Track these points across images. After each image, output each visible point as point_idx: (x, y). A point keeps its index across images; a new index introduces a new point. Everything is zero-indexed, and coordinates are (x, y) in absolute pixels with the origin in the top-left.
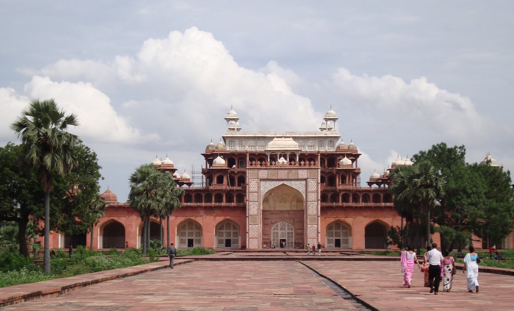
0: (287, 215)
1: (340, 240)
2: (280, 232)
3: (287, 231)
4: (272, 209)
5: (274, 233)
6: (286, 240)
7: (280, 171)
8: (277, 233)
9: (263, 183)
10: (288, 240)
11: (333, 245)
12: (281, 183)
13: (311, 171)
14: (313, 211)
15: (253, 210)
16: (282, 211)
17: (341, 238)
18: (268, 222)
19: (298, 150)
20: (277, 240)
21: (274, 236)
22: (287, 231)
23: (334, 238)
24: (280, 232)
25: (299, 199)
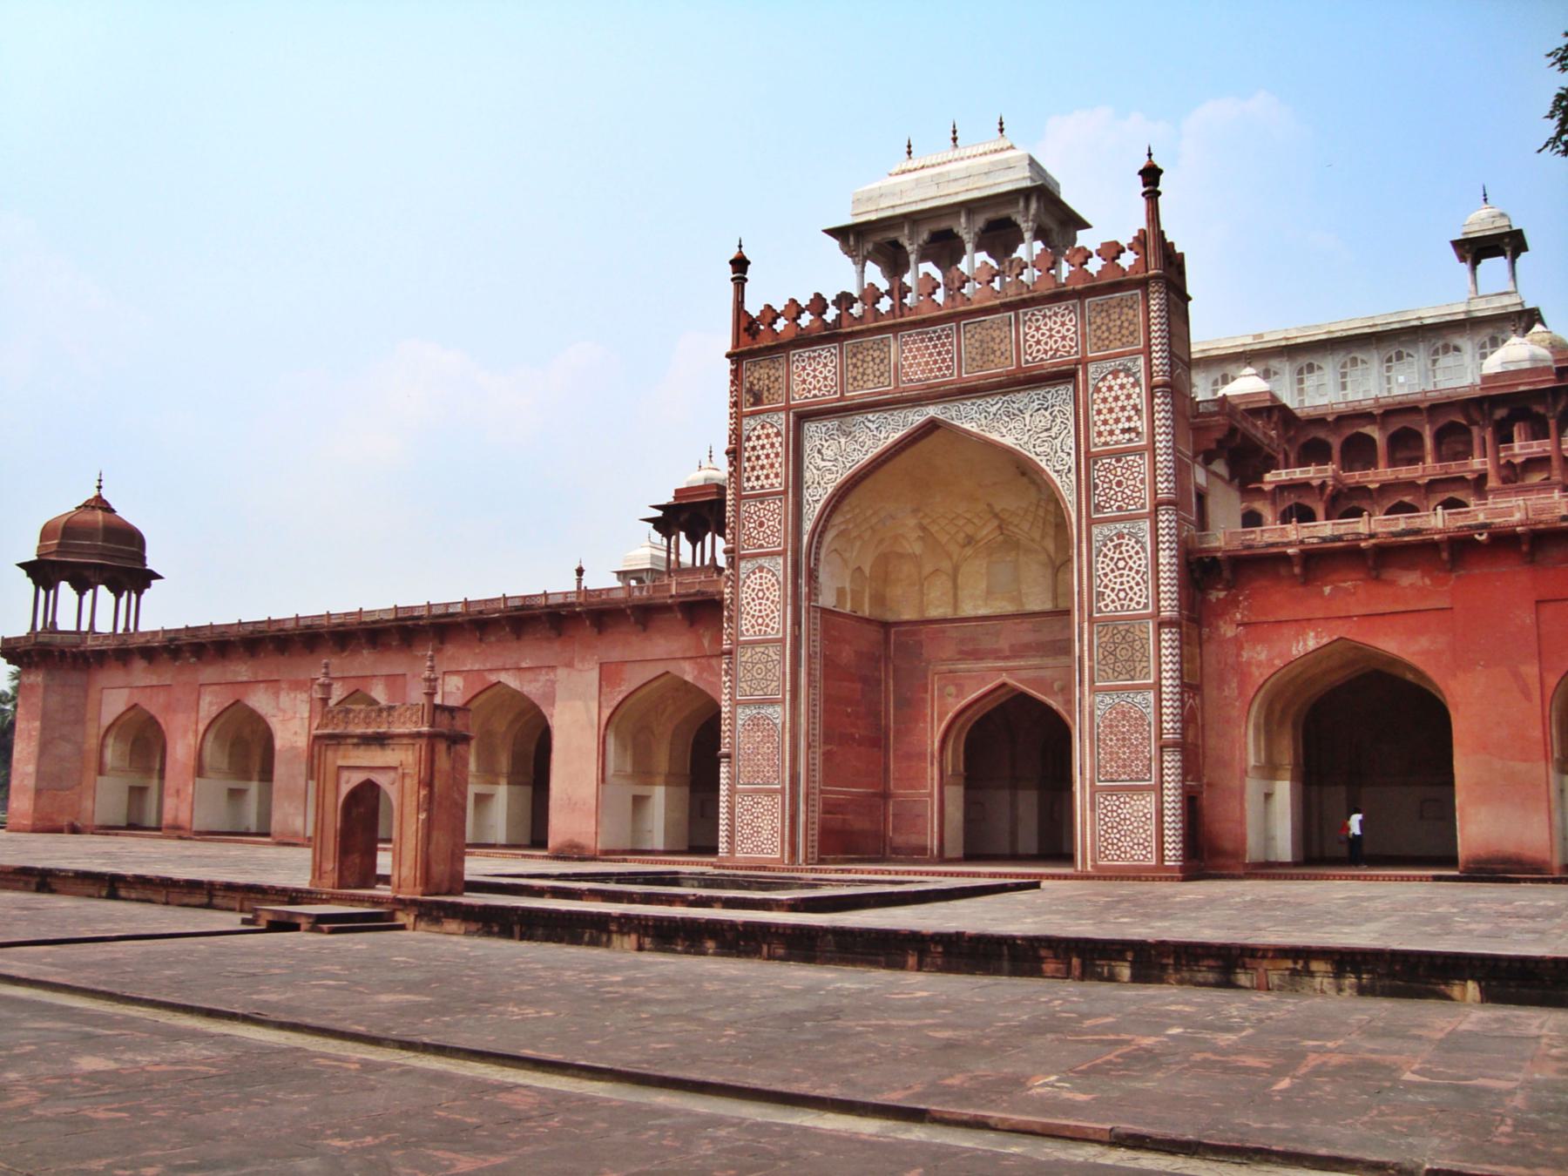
19: (1024, 194)
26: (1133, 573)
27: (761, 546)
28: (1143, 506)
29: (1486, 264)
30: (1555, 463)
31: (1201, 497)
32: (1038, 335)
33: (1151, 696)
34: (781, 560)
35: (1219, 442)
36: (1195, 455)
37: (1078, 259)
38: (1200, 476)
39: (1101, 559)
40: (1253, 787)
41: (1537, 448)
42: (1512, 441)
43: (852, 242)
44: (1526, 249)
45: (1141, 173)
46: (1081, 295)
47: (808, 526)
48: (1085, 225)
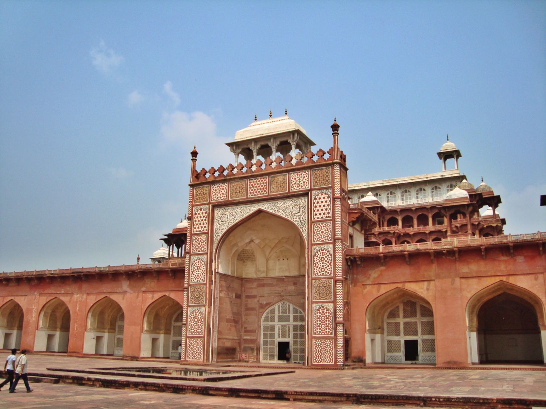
0: (292, 288)
1: (416, 341)
2: (277, 325)
3: (292, 323)
4: (263, 275)
5: (266, 328)
6: (291, 344)
7: (253, 182)
8: (272, 328)
9: (218, 212)
10: (295, 343)
11: (401, 355)
12: (254, 208)
13: (318, 172)
14: (323, 270)
15: (196, 273)
16: (281, 280)
17: (419, 338)
18: (253, 303)
20: (272, 343)
21: (265, 335)
22: (292, 323)
23: (402, 339)
24: (277, 325)
25: (293, 241)
26: (327, 263)
27: (199, 251)
28: (331, 240)
29: (448, 160)
30: (469, 227)
31: (351, 237)
32: (295, 181)
33: (332, 305)
34: (205, 256)
35: (357, 218)
36: (349, 223)
37: (309, 155)
38: (351, 230)
39: (316, 257)
40: (368, 337)
41: (464, 221)
42: (456, 218)
43: (234, 148)
44: (461, 156)
45: (332, 127)
46: (310, 168)
47: (215, 245)
48: (312, 144)
